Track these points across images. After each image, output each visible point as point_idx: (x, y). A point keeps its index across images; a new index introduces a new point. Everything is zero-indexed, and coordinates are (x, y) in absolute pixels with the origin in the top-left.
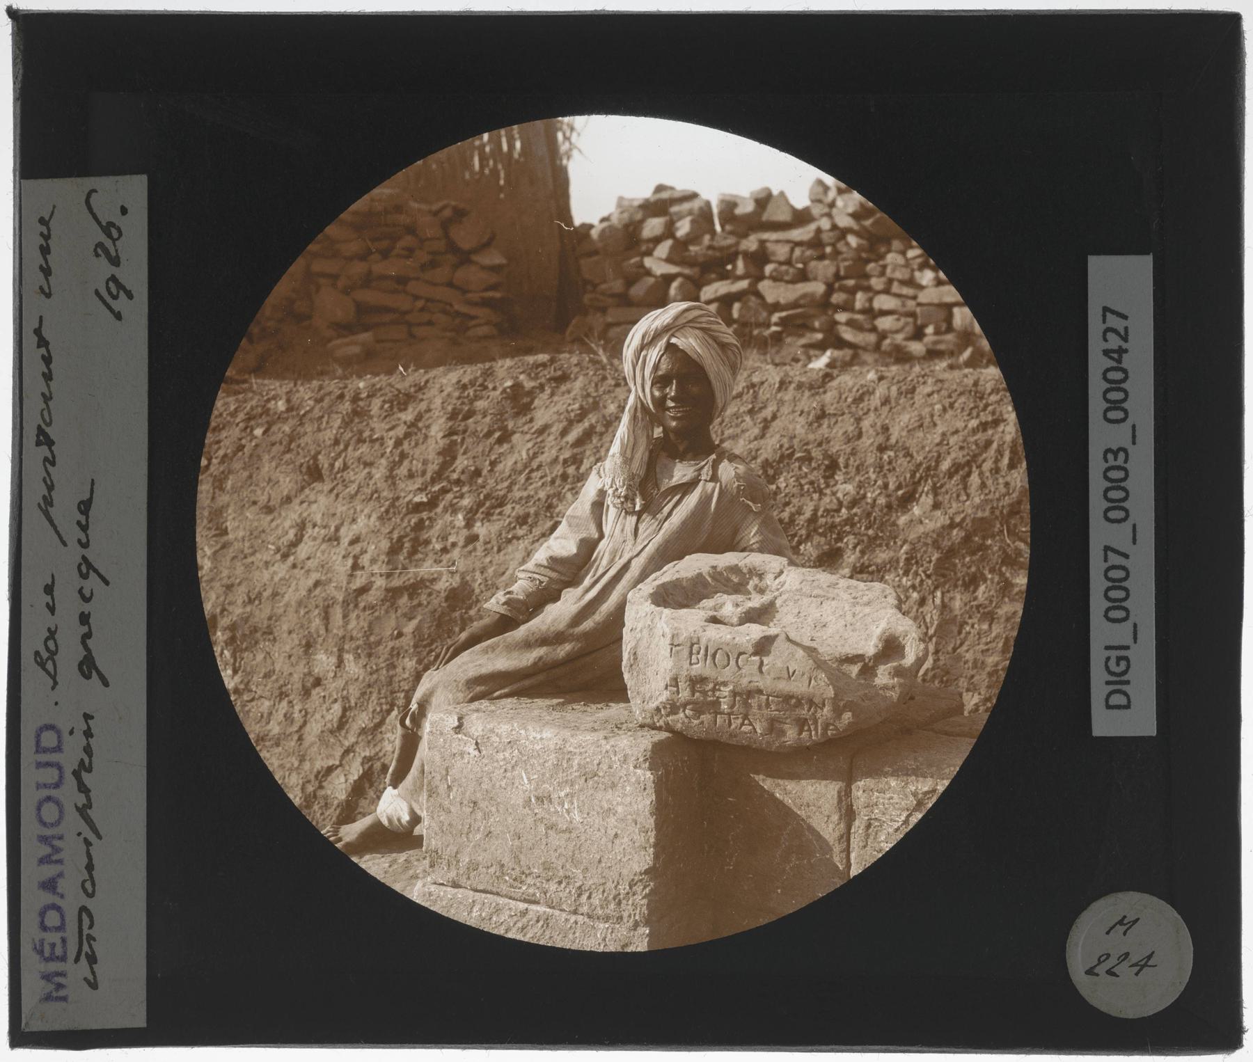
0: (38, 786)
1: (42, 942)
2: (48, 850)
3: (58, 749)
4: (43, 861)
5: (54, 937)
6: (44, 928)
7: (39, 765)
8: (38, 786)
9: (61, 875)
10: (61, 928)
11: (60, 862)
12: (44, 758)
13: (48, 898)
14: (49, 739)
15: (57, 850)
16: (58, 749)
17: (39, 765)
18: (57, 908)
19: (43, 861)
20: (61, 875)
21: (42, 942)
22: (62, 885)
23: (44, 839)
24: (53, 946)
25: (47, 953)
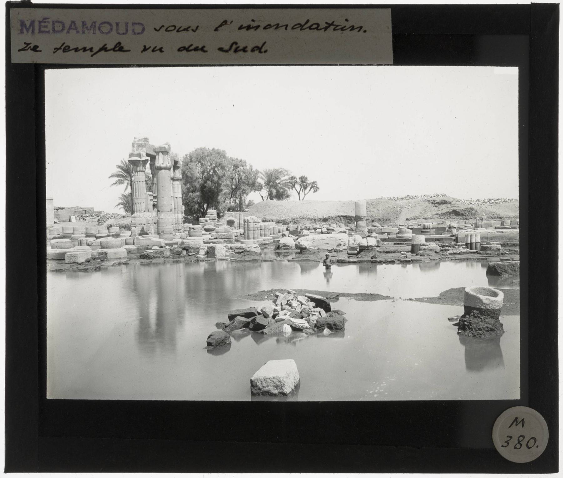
0: (117, 24)
1: (49, 22)
4: (84, 23)
7: (127, 24)
8: (117, 24)
10: (54, 31)
13: (67, 26)
17: (127, 24)
19: (84, 23)
20: (78, 32)
21: (49, 22)
22: (73, 32)
24: (46, 27)
25: (46, 24)
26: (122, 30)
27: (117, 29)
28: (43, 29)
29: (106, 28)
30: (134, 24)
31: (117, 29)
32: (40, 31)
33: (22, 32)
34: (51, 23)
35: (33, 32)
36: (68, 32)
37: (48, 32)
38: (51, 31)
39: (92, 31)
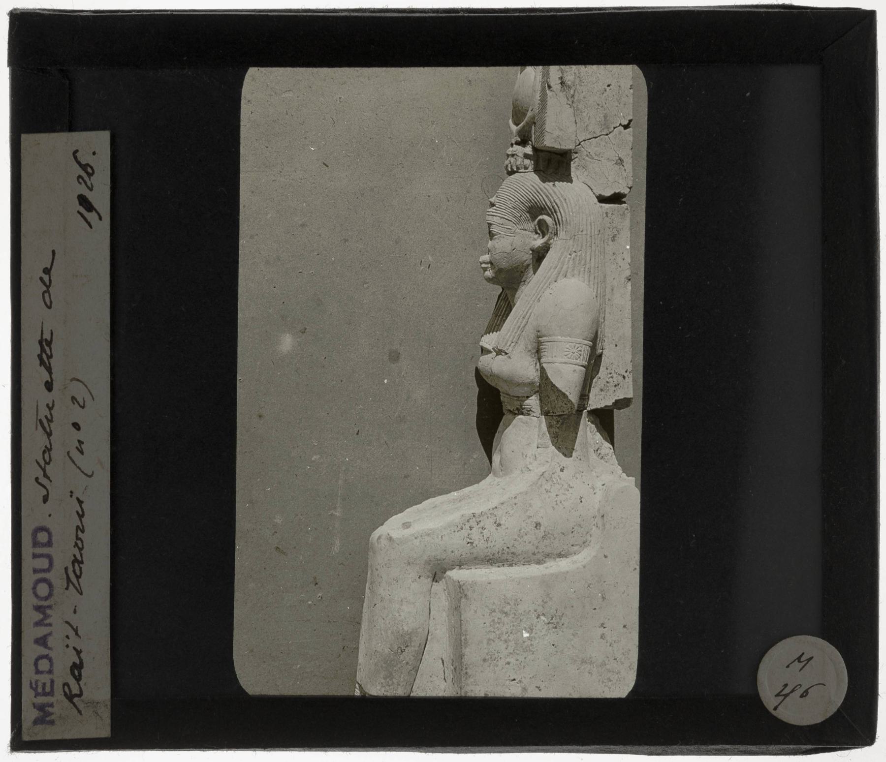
0: (35, 571)
1: (37, 682)
2: (41, 616)
3: (49, 544)
4: (38, 624)
5: (45, 678)
6: (38, 672)
7: (35, 556)
8: (35, 571)
9: (50, 634)
10: (50, 672)
11: (50, 625)
12: (39, 551)
13: (42, 651)
14: (43, 537)
15: (46, 616)
16: (49, 544)
18: (46, 657)
19: (38, 624)
20: (50, 634)
21: (37, 682)
22: (51, 642)
23: (38, 608)
26: (43, 563)
27: (44, 571)
28: (48, 689)
29: (43, 590)
30: (36, 544)
31: (44, 571)
32: (51, 693)
33: (52, 723)
34: (38, 677)
35: (51, 705)
36: (50, 649)
37: (52, 682)
38: (51, 676)
39: (48, 612)
